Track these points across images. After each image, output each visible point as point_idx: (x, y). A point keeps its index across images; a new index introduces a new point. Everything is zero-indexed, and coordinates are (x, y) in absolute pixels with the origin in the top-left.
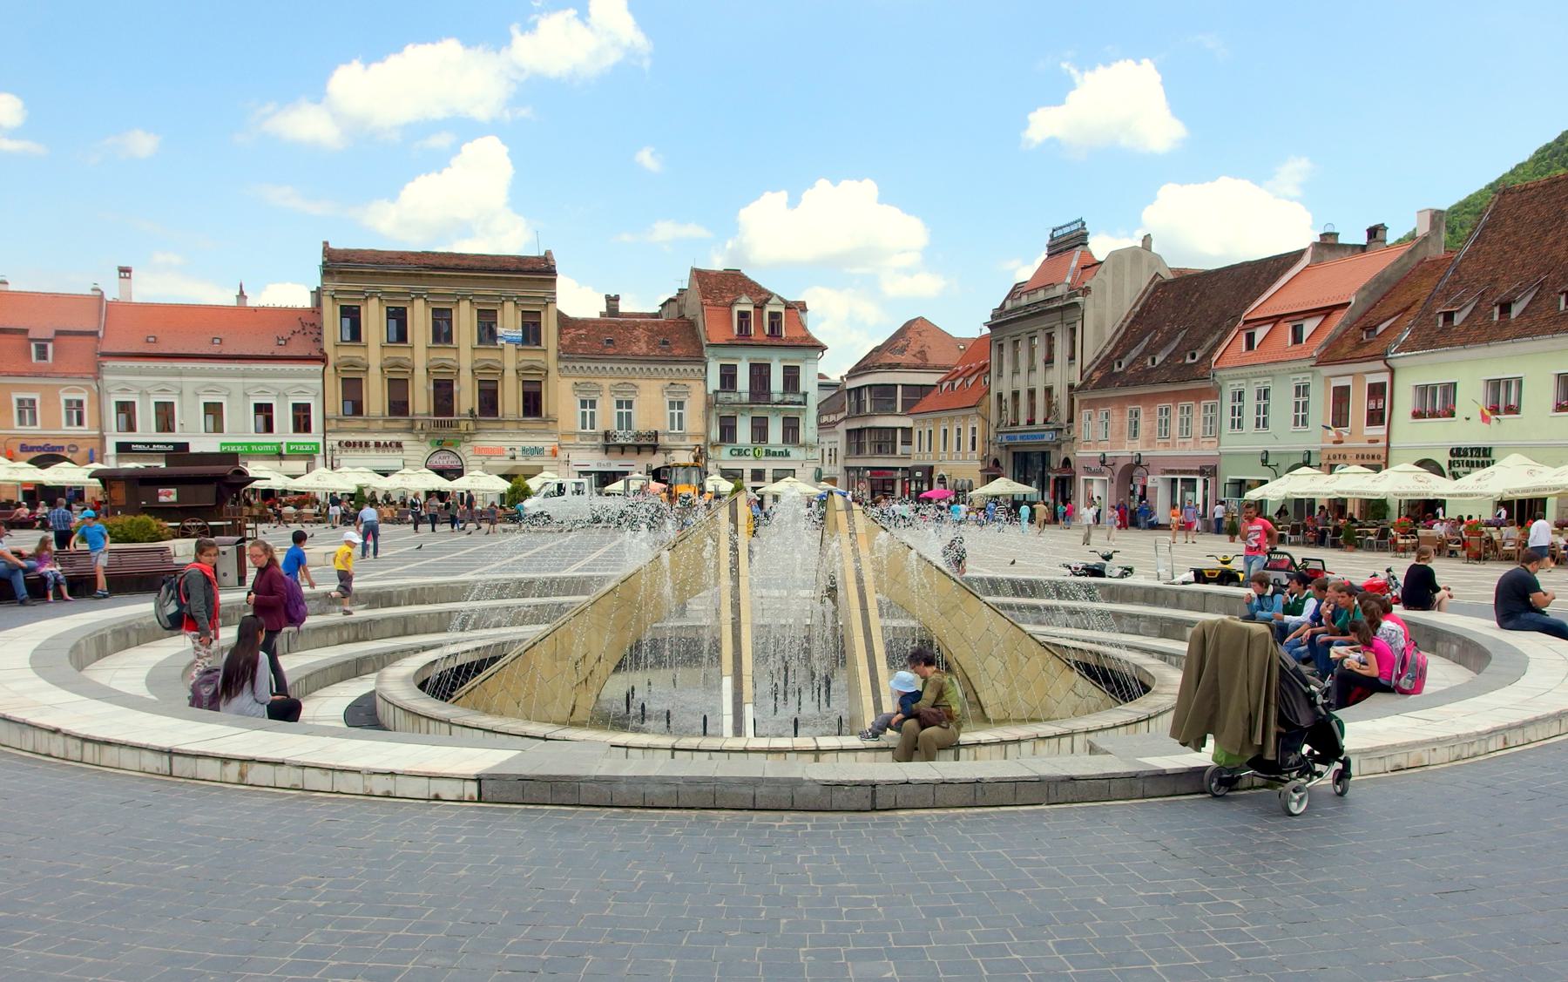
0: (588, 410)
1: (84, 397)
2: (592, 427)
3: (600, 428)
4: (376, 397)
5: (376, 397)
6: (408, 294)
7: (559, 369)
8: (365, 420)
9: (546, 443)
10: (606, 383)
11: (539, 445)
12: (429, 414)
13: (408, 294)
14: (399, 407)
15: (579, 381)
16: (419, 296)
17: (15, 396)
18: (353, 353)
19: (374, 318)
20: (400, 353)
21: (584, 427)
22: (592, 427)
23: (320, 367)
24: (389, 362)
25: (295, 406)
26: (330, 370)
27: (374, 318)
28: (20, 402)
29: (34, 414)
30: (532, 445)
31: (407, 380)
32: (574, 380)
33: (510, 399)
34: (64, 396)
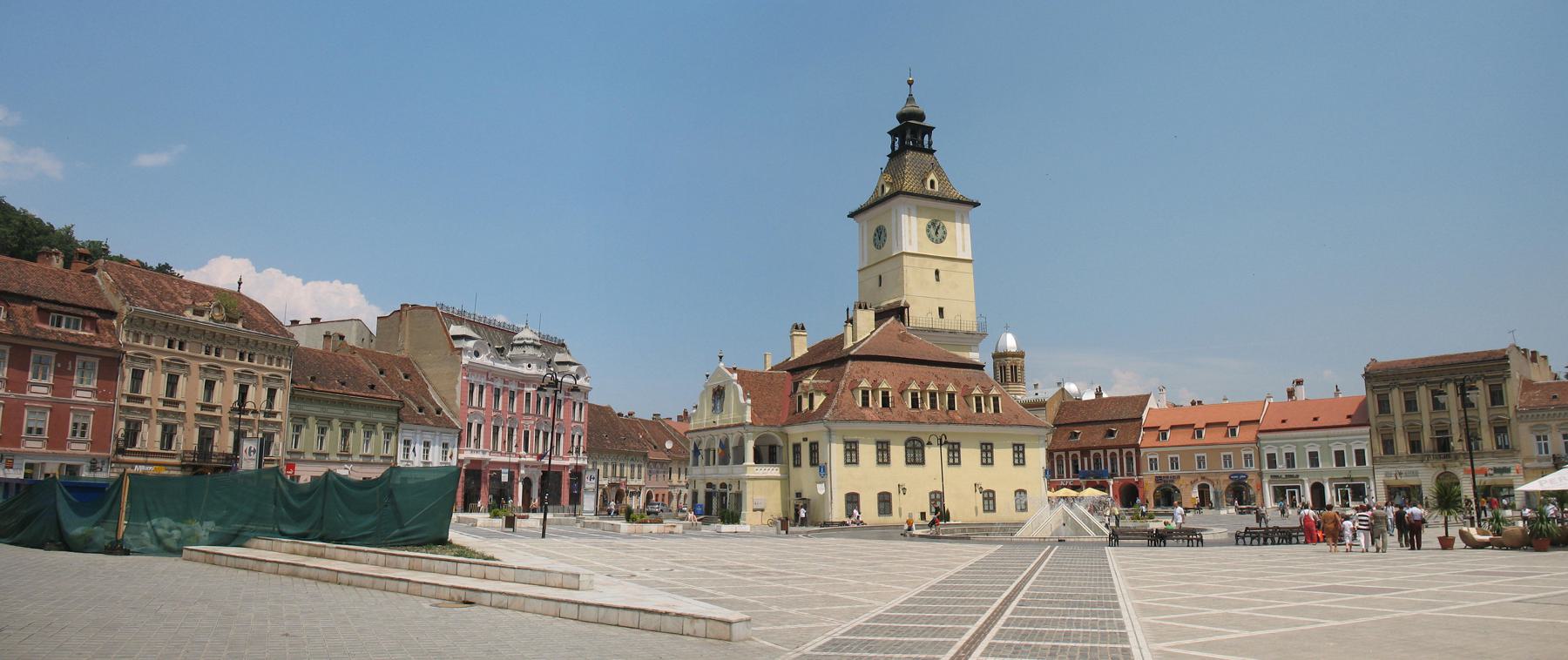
0: (1543, 442)
1: (1252, 452)
2: (1547, 452)
3: (1551, 453)
4: (1402, 446)
5: (1402, 446)
6: (1415, 384)
7: (1518, 418)
8: (1396, 457)
9: (1514, 466)
10: (1553, 424)
11: (1508, 466)
12: (1434, 451)
13: (1415, 384)
14: (1415, 446)
15: (1533, 424)
16: (1422, 384)
17: (1222, 454)
18: (1385, 419)
19: (1396, 399)
20: (1413, 417)
21: (1541, 453)
22: (1547, 452)
23: (1367, 429)
24: (1408, 423)
25: (1357, 451)
26: (1374, 431)
27: (1396, 399)
28: (1225, 456)
29: (1230, 463)
30: (1502, 466)
31: (1419, 432)
32: (1529, 424)
33: (1487, 440)
34: (1243, 453)
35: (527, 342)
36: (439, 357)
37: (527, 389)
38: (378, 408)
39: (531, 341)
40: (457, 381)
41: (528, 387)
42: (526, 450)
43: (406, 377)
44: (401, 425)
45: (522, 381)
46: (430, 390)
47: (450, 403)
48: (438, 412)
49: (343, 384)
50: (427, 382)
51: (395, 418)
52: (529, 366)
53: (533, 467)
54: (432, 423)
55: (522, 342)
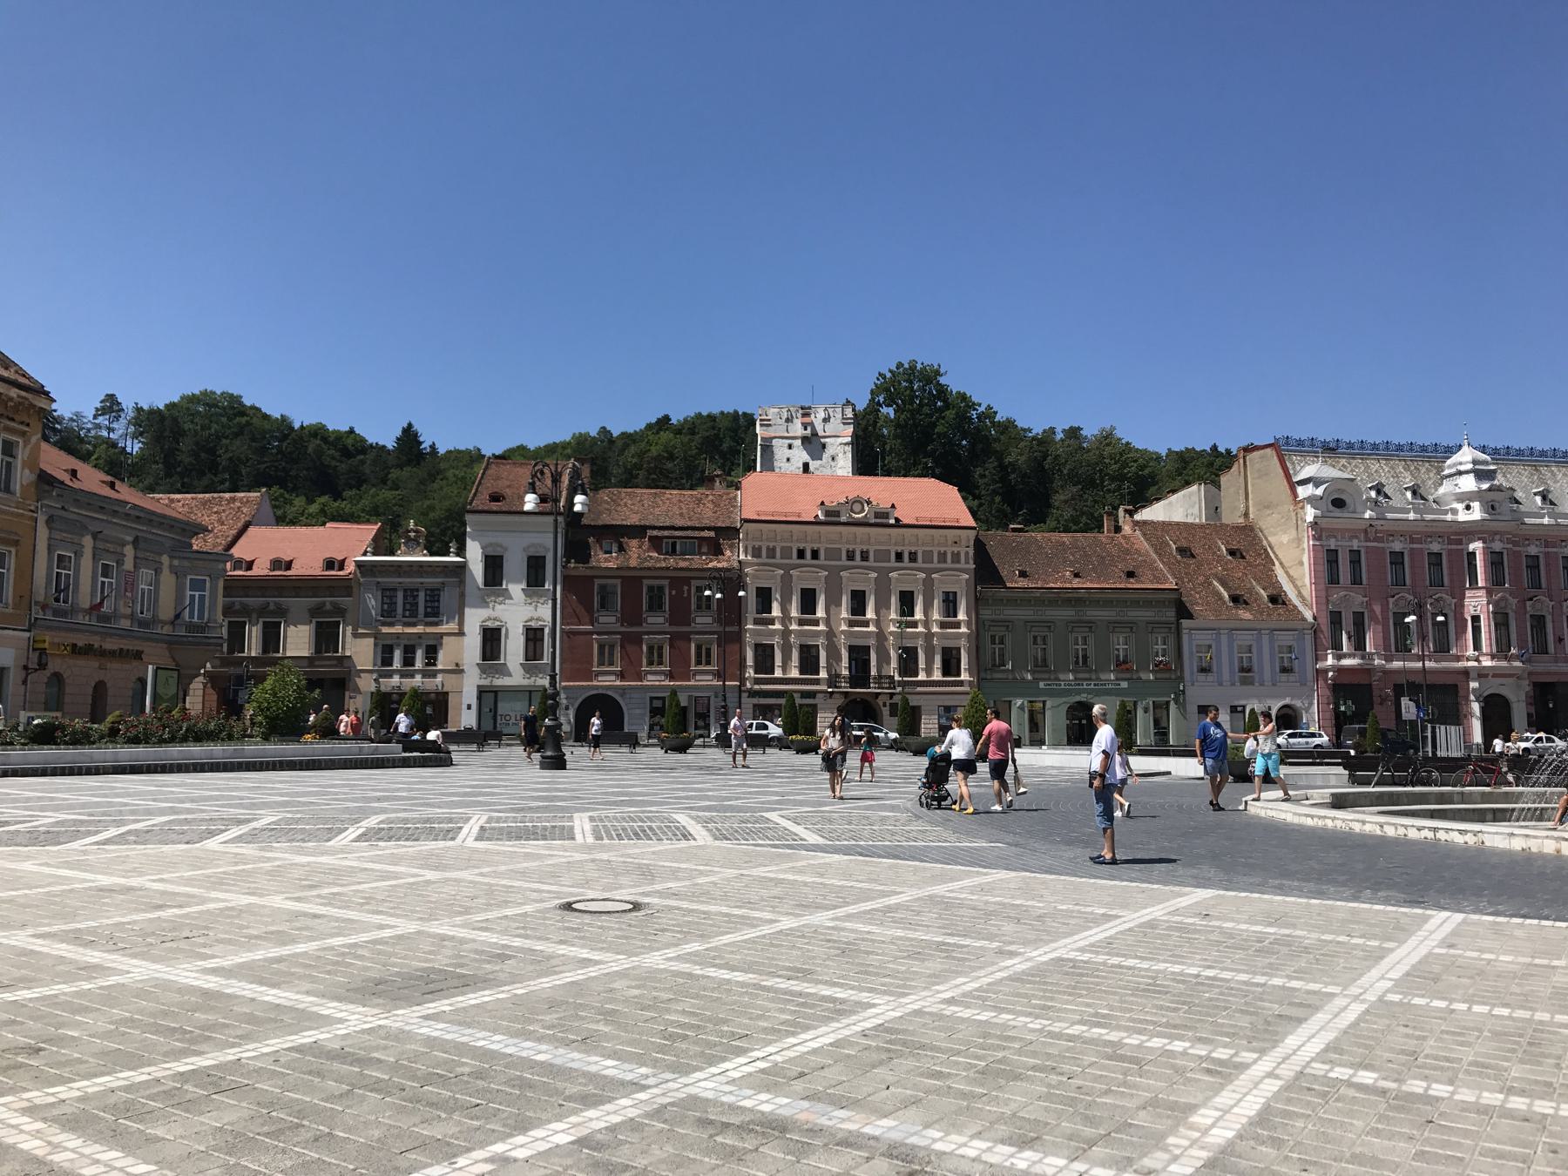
35: (1462, 468)
36: (1283, 517)
37: (1472, 547)
38: (1136, 604)
39: (1470, 466)
40: (1304, 549)
41: (1473, 541)
42: (1477, 647)
43: (1232, 553)
44: (1185, 623)
45: (1456, 534)
46: (1276, 563)
47: (1299, 583)
48: (1274, 599)
49: (1077, 575)
50: (1273, 557)
51: (1173, 614)
52: (1468, 508)
53: (1495, 676)
54: (1251, 617)
55: (1453, 470)
